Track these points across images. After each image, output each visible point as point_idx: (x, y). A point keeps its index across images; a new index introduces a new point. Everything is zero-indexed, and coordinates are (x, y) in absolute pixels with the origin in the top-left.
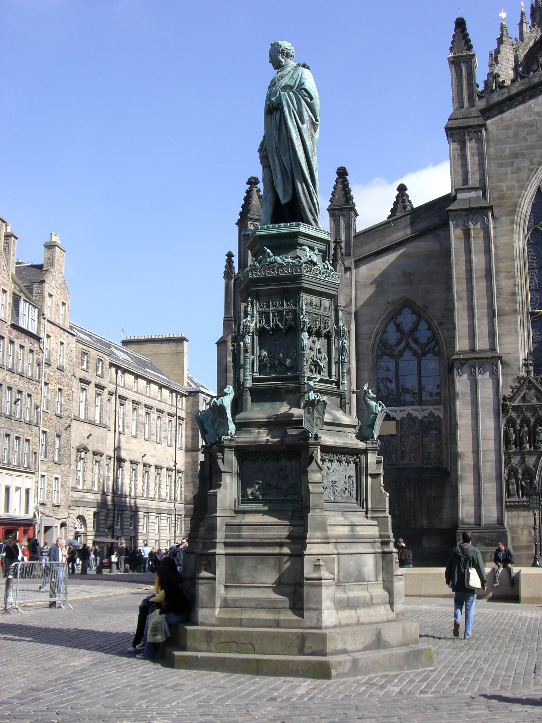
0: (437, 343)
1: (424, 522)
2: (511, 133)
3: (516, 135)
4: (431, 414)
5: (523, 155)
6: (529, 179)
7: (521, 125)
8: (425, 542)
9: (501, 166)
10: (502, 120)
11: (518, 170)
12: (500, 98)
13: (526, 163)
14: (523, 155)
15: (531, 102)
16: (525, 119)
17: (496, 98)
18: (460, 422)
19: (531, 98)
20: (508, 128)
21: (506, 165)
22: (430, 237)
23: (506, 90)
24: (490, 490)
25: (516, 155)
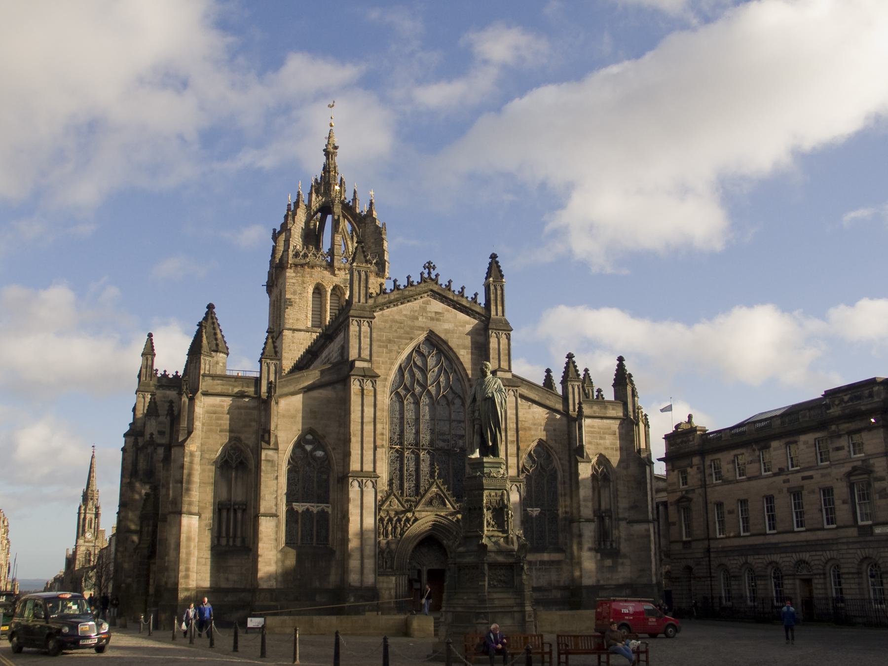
0: (329, 462)
1: (317, 584)
2: (388, 325)
3: (391, 327)
4: (323, 510)
5: (394, 342)
6: (396, 359)
7: (394, 321)
8: (318, 598)
9: (380, 347)
10: (382, 315)
11: (391, 351)
12: (383, 301)
13: (395, 348)
14: (394, 342)
15: (401, 307)
16: (397, 317)
17: (381, 300)
18: (352, 518)
19: (402, 303)
20: (386, 321)
21: (383, 347)
22: (330, 388)
23: (387, 296)
24: (369, 564)
25: (390, 341)
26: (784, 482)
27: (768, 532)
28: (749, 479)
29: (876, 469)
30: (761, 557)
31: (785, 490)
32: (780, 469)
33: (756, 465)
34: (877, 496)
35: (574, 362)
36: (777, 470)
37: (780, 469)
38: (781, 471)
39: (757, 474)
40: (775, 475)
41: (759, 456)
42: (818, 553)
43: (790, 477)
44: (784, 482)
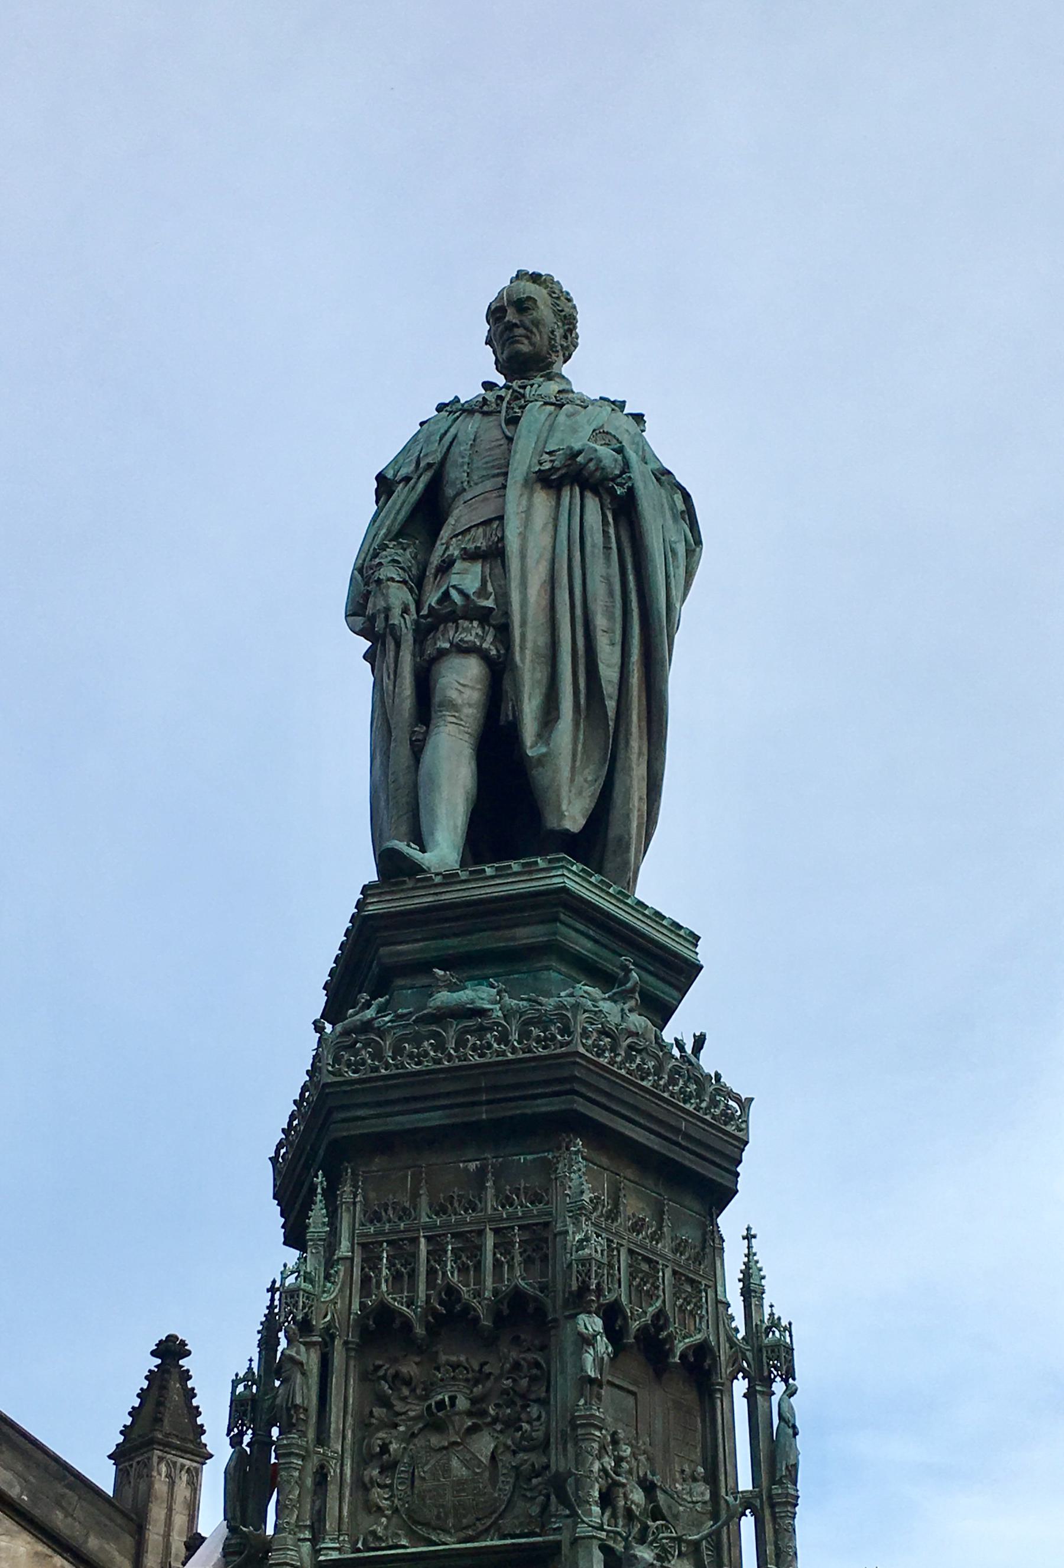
35: (186, 1376)
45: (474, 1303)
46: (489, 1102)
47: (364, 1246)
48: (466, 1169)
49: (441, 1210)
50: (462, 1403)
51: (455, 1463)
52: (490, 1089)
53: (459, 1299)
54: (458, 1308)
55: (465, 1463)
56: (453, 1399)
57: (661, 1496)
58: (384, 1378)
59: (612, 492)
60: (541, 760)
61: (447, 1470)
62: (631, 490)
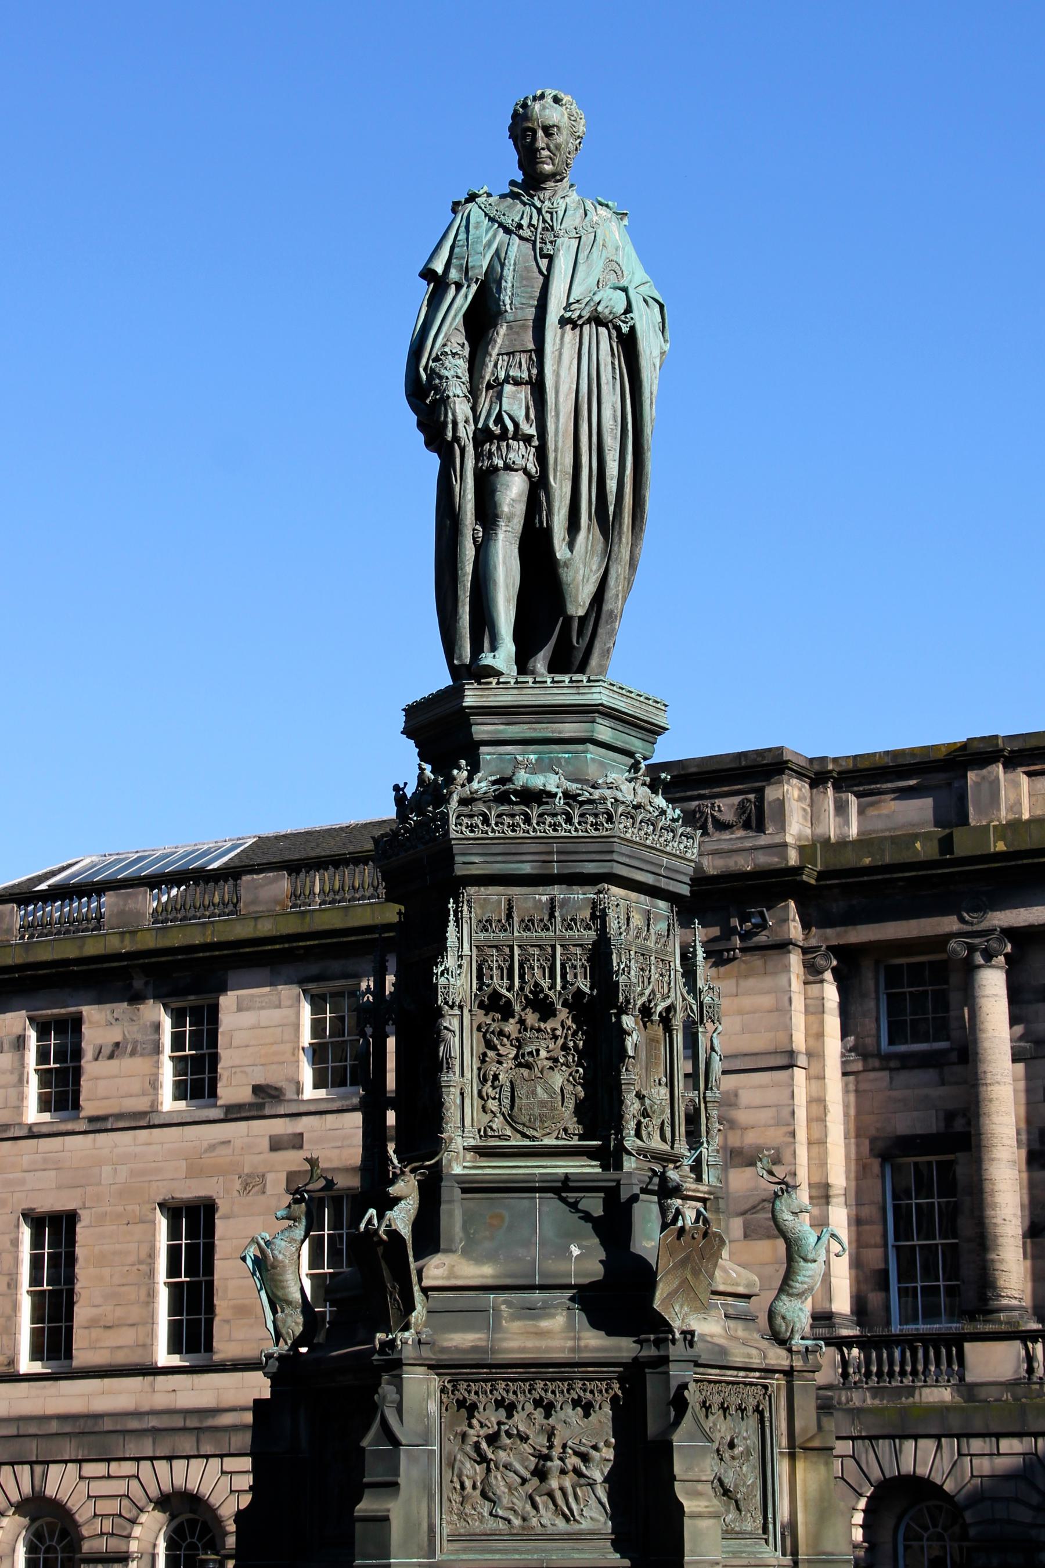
26: (276, 1145)
27: (26, 1365)
28: (99, 1124)
29: (742, 1116)
30: (128, 1468)
31: (277, 1185)
32: (258, 1089)
33: (137, 1065)
34: (736, 1226)
36: (244, 1095)
37: (258, 1089)
38: (266, 1099)
39: (141, 1104)
40: (235, 1113)
41: (157, 1027)
42: (115, 1468)
43: (303, 1125)
44: (276, 1145)
45: (551, 993)
46: (551, 853)
47: (477, 947)
48: (540, 900)
49: (527, 929)
50: (543, 1054)
51: (539, 1090)
52: (559, 853)
53: (542, 991)
54: (541, 996)
55: (546, 1090)
56: (538, 1051)
57: (647, 1101)
58: (493, 1032)
59: (618, 329)
60: (566, 565)
61: (534, 1093)
62: (633, 329)
